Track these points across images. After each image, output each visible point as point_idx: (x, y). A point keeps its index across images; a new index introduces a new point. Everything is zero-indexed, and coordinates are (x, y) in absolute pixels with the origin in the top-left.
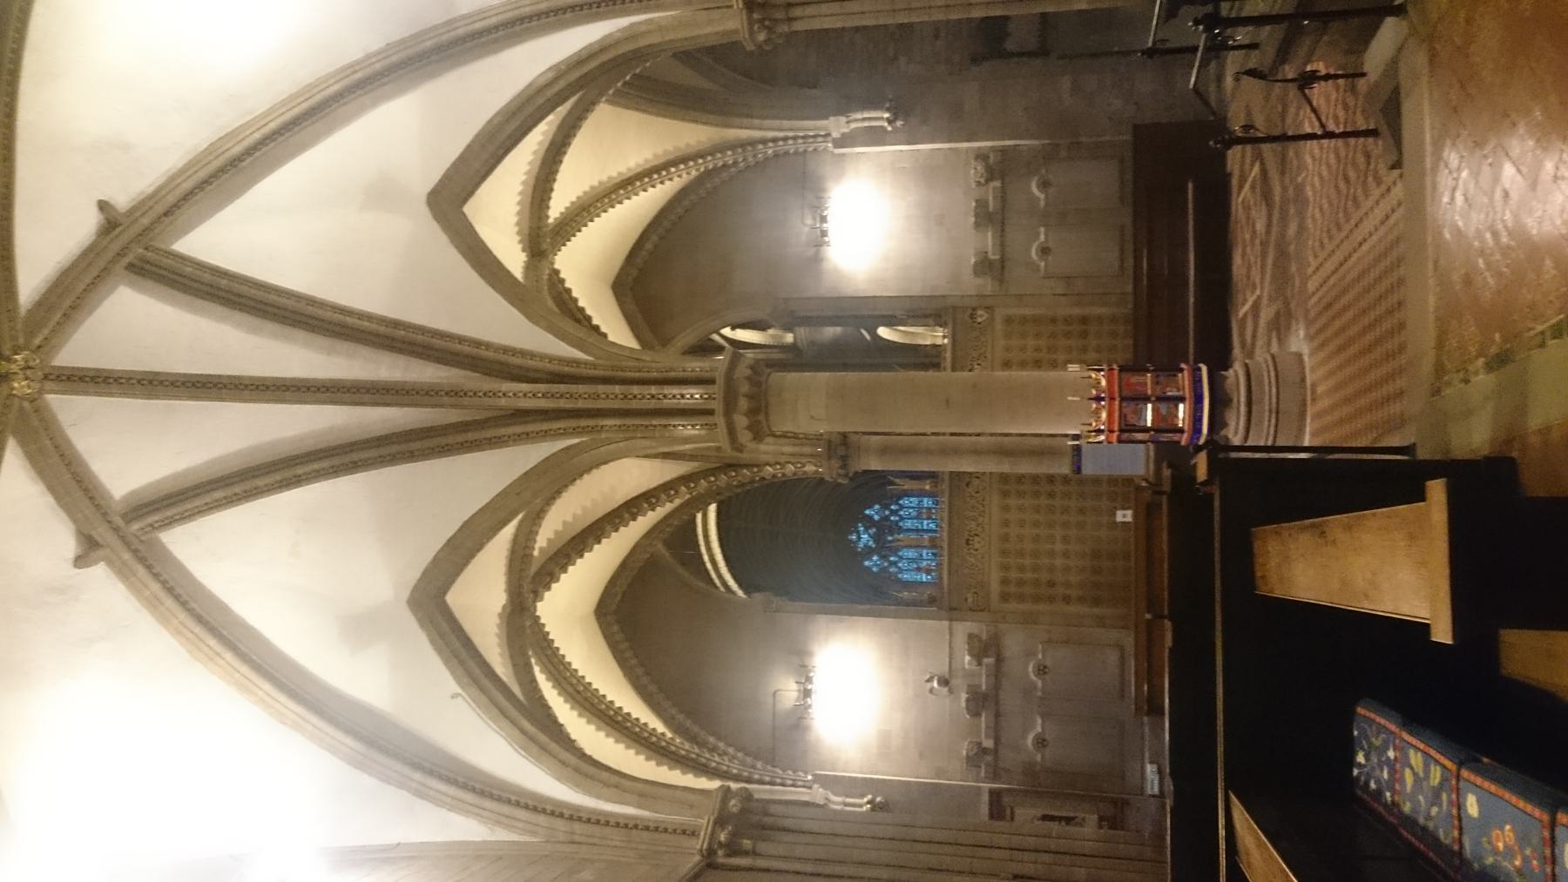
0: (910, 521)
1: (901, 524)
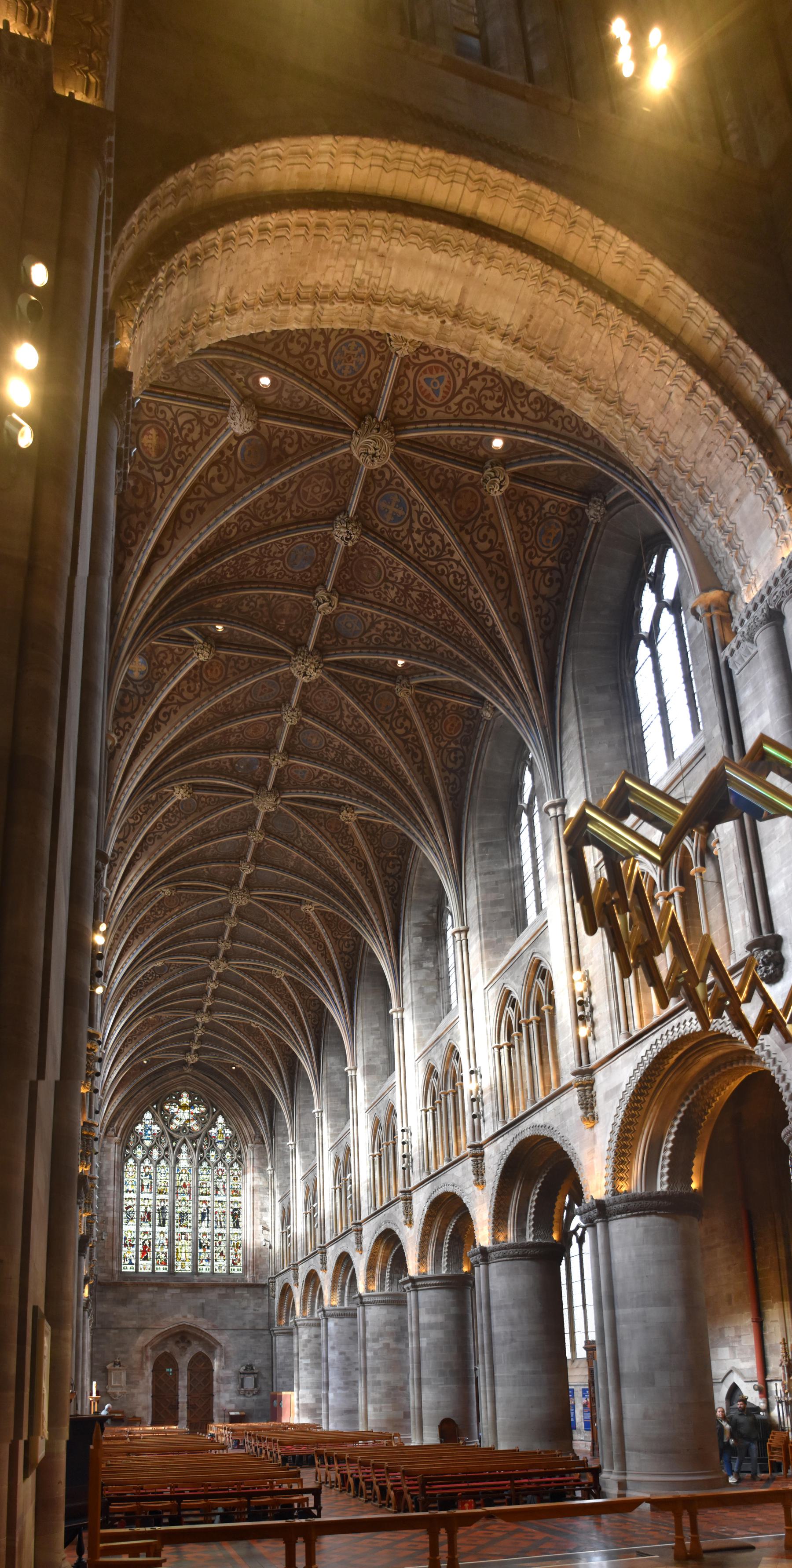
1: (205, 1165)
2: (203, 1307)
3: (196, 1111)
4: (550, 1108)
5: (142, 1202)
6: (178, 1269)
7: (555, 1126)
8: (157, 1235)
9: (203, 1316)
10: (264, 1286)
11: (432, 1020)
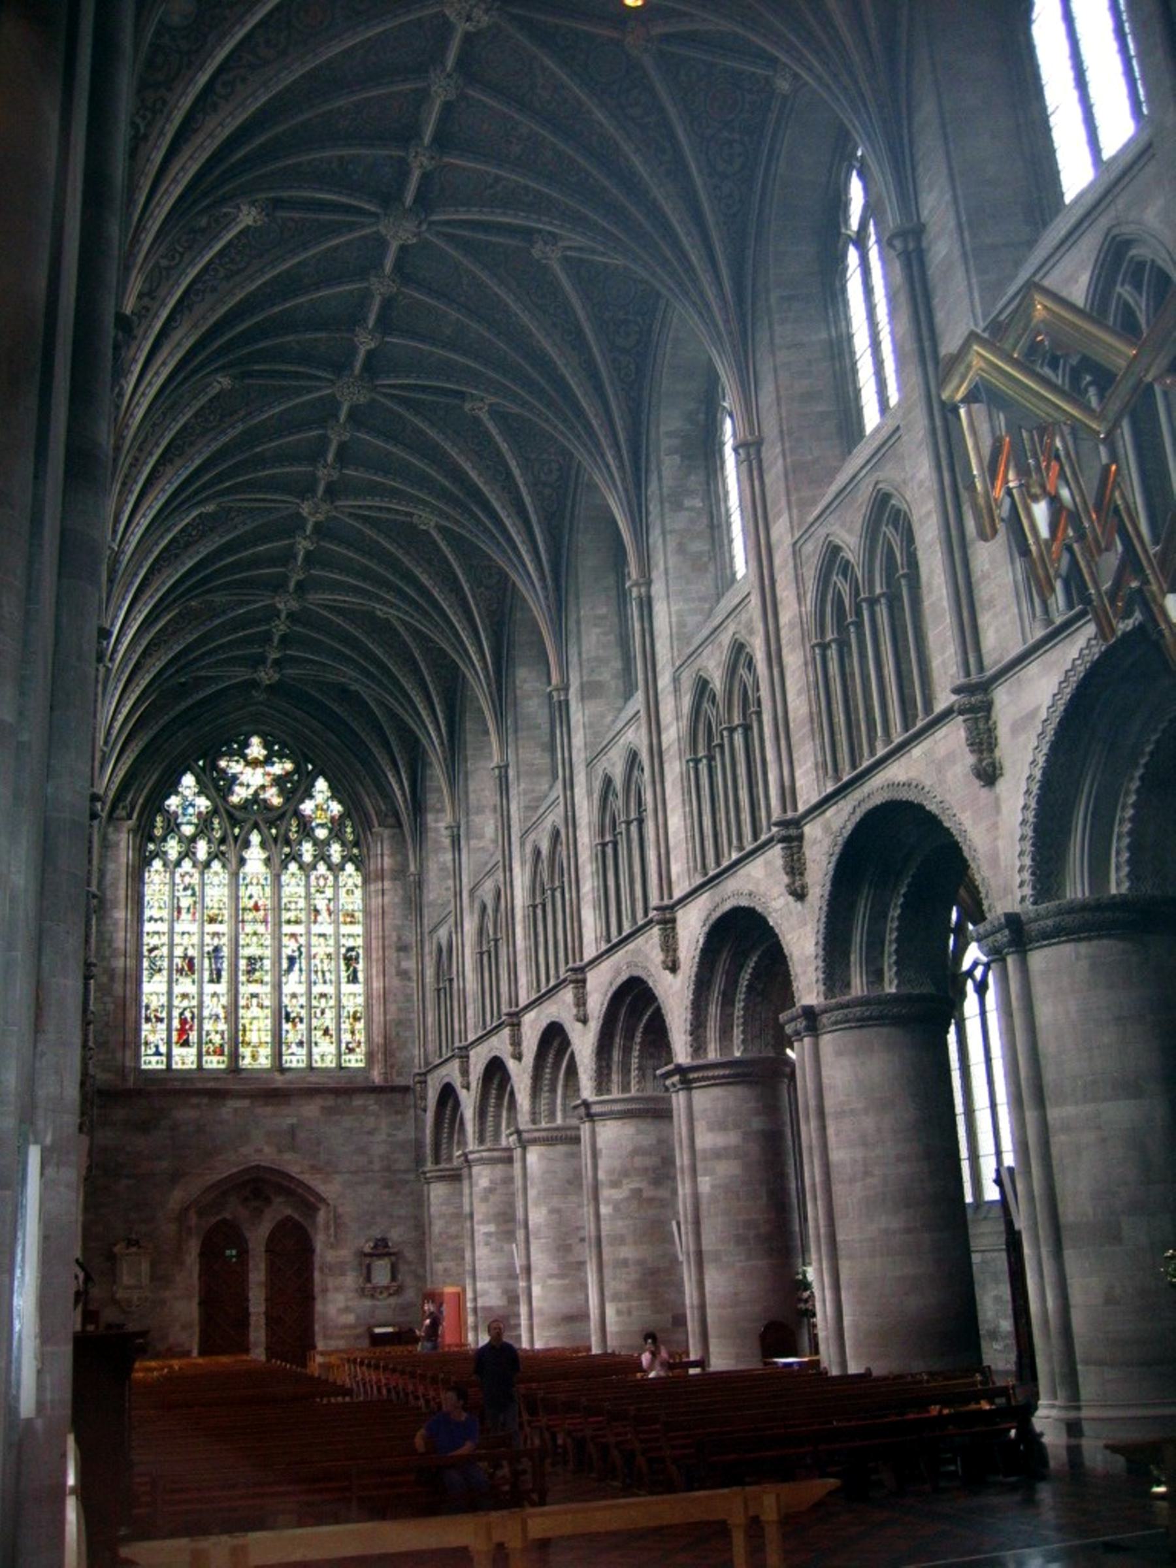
0: (301, 891)
2: (292, 1131)
3: (278, 769)
4: (917, 751)
5: (177, 939)
6: (246, 1063)
7: (928, 783)
8: (207, 1000)
9: (293, 1148)
10: (406, 1089)
11: (703, 599)
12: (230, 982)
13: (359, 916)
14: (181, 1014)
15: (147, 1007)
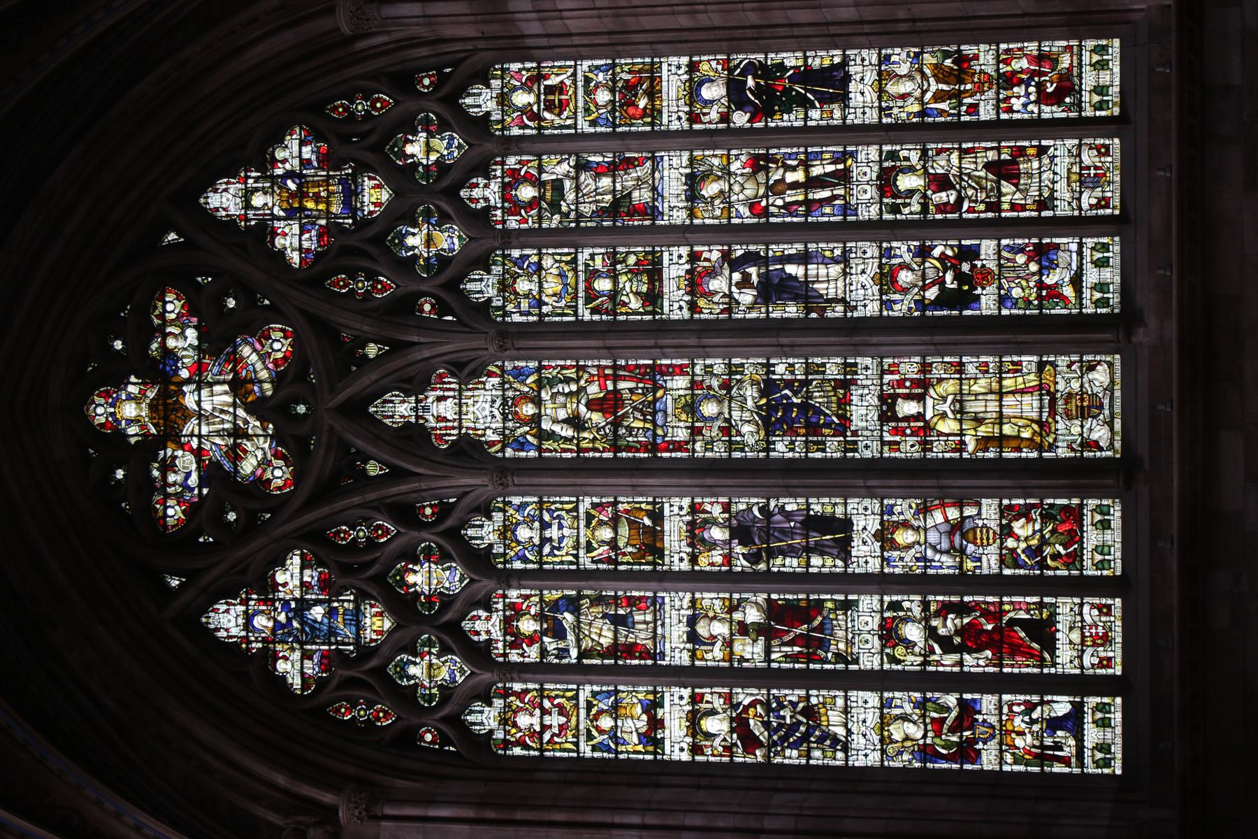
1: (483, 286)
8: (903, 563)
12: (846, 493)
13: (627, 67)
14: (947, 645)
15: (926, 752)
